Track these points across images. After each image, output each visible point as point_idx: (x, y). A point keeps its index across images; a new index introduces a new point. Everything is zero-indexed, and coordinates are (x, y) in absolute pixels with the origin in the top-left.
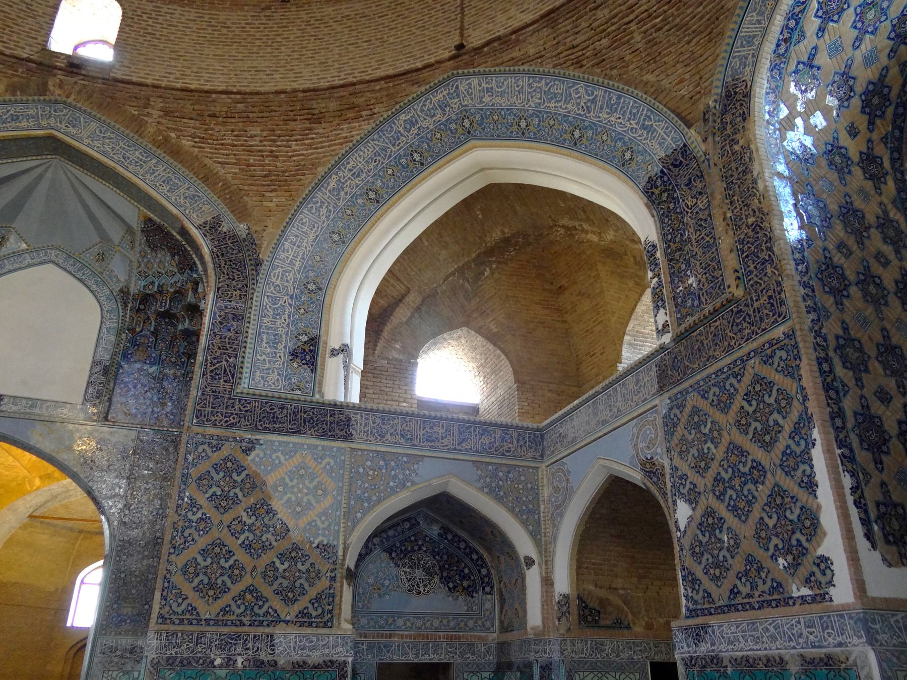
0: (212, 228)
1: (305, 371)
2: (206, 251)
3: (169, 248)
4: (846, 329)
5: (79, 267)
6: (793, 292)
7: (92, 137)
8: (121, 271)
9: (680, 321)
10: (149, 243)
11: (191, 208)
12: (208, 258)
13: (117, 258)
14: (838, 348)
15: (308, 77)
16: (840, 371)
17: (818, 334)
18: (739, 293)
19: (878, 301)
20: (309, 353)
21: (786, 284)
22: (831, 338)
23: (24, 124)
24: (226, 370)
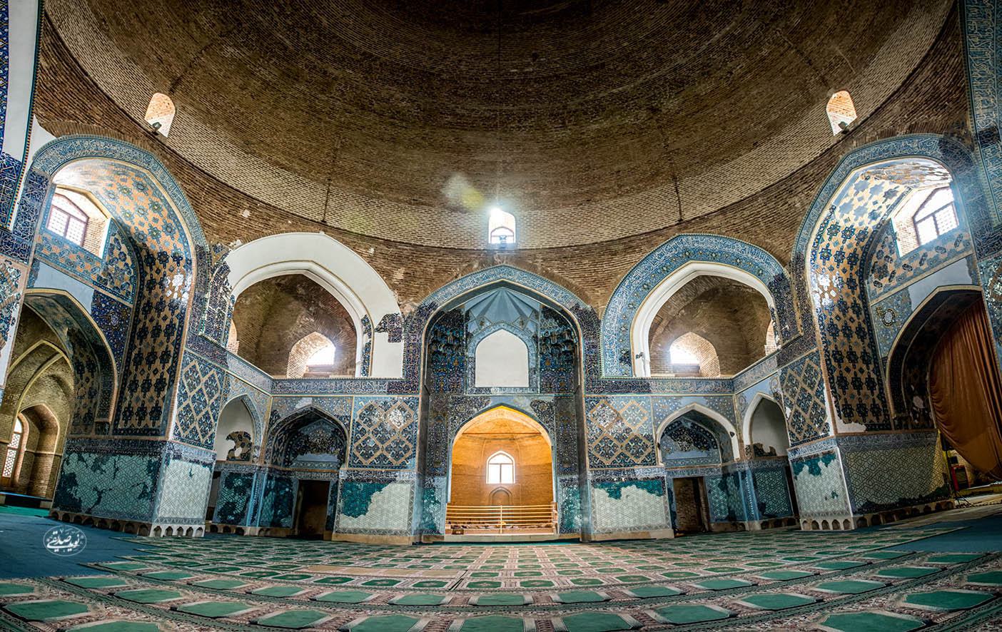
0: (576, 309)
1: (627, 366)
2: (575, 319)
3: (555, 318)
4: (836, 348)
5: (510, 326)
6: (819, 336)
7: (518, 278)
8: (531, 328)
9: (784, 341)
10: (545, 317)
11: (562, 299)
12: (577, 323)
13: (530, 323)
14: (834, 355)
15: (606, 234)
16: (833, 363)
17: (826, 351)
18: (802, 334)
19: (848, 336)
20: (626, 358)
21: (817, 333)
22: (831, 352)
23: (491, 279)
24: (593, 370)
